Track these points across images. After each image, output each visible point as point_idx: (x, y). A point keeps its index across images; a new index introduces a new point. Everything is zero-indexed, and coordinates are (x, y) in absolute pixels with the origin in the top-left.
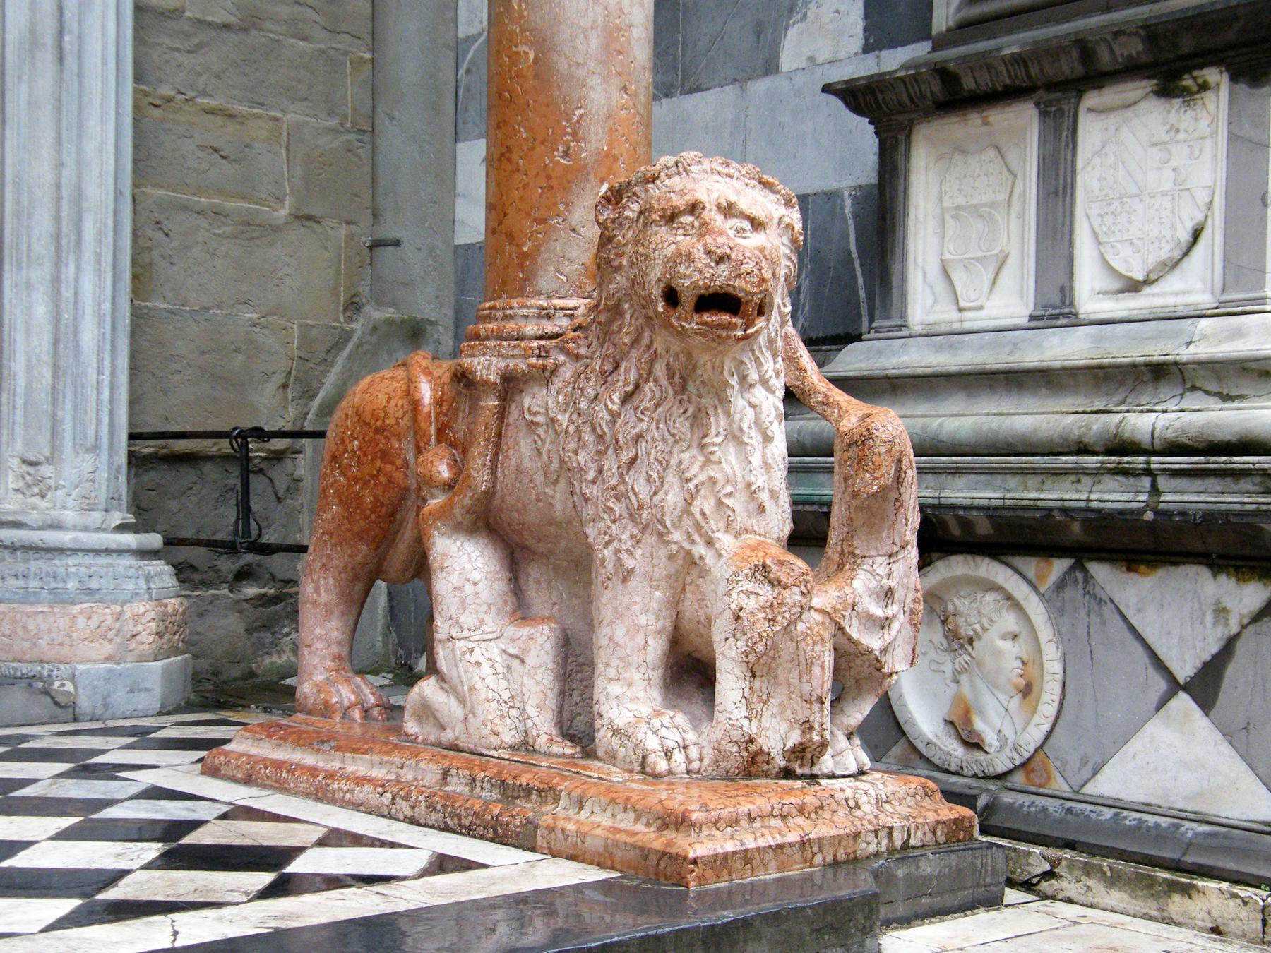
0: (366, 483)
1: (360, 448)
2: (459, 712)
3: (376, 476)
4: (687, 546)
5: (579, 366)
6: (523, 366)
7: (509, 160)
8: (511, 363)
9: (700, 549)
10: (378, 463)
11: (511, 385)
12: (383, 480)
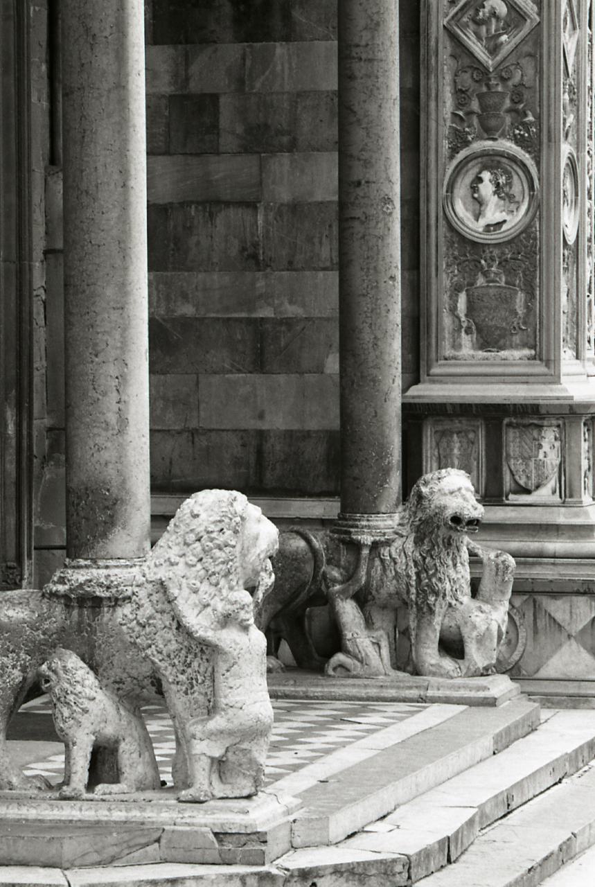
0: (286, 580)
1: (283, 566)
2: (359, 664)
3: (293, 578)
4: (450, 601)
5: (404, 539)
6: (383, 539)
7: (367, 463)
8: (378, 538)
9: (454, 602)
10: (294, 572)
11: (375, 546)
12: (296, 579)
